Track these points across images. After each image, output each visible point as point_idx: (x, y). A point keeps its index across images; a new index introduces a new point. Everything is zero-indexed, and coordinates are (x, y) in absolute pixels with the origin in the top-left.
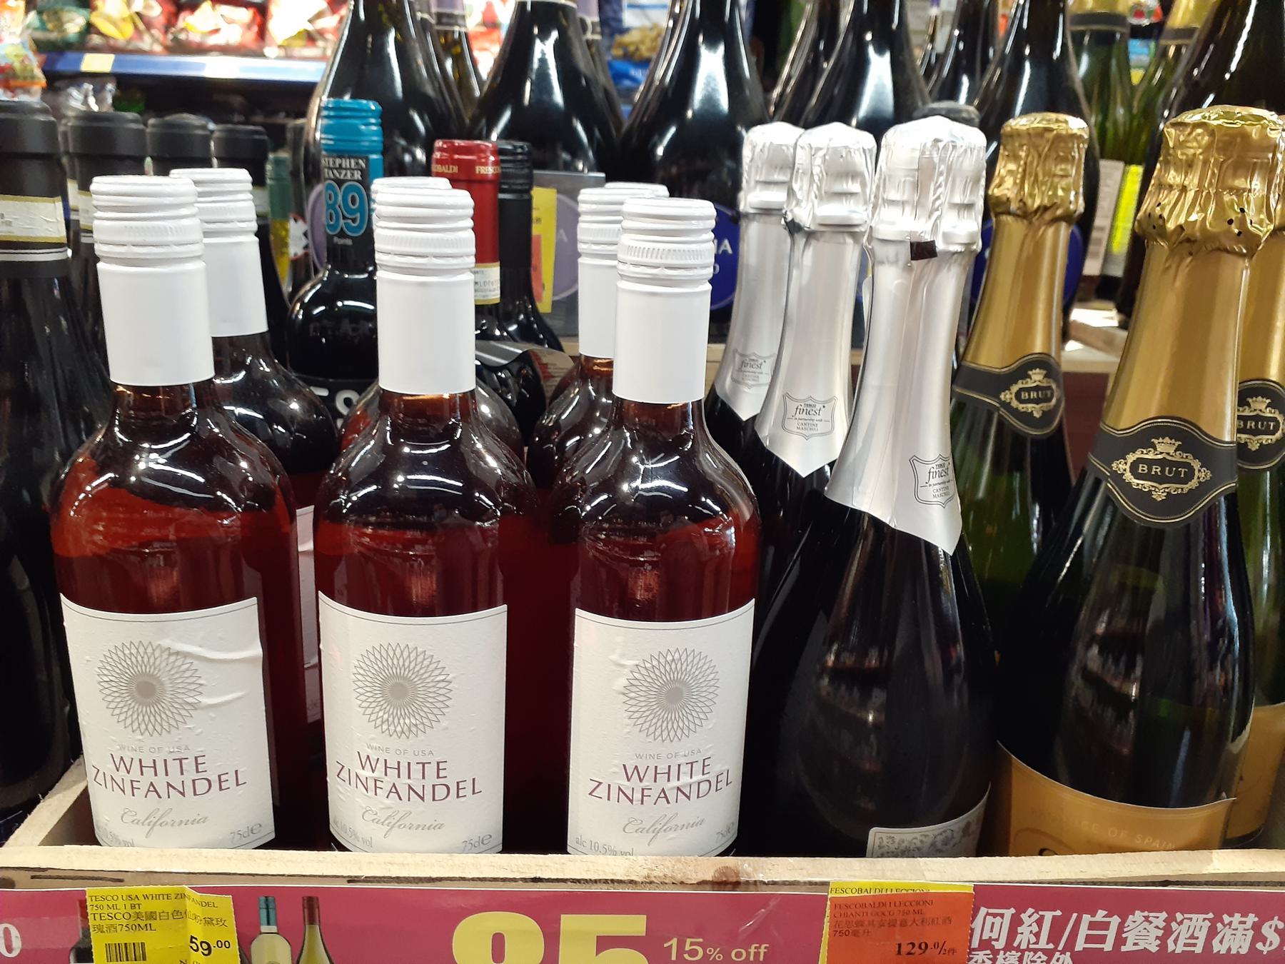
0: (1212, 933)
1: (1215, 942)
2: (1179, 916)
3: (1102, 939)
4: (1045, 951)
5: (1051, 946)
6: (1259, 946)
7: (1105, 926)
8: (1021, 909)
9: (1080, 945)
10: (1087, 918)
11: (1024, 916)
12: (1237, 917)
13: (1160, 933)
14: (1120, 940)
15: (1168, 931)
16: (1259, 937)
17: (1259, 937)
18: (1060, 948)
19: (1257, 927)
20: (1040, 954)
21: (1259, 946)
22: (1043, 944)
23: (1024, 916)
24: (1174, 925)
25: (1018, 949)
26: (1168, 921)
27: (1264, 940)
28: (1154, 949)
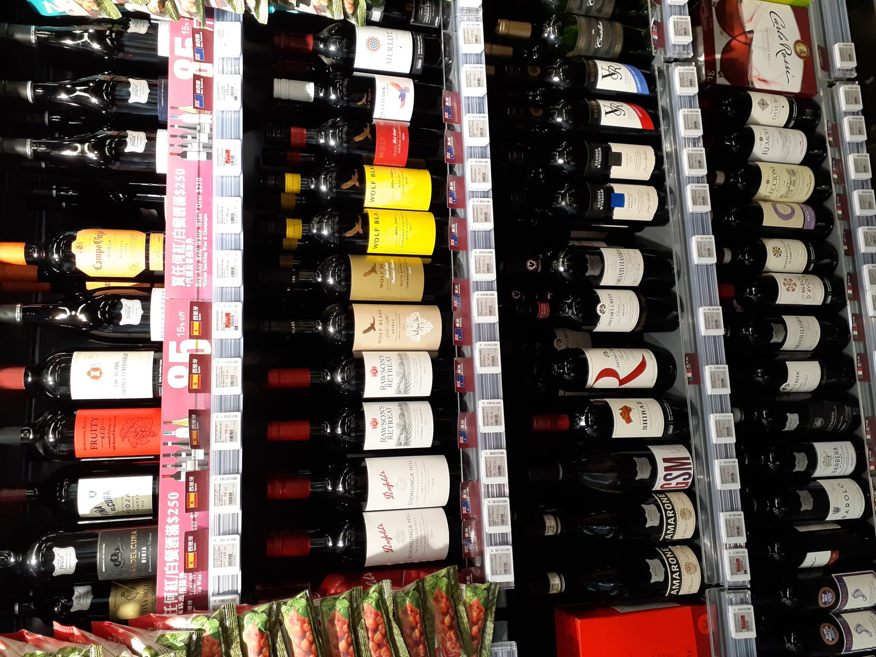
0: (172, 536)
1: (175, 535)
2: (166, 547)
3: (174, 566)
4: (179, 581)
5: (177, 580)
6: (176, 522)
7: (170, 567)
8: (165, 591)
9: (177, 572)
10: (167, 572)
11: (167, 590)
12: (166, 531)
13: (172, 550)
14: (175, 561)
15: (172, 548)
16: (174, 523)
17: (174, 523)
18: (177, 577)
19: (170, 525)
20: (179, 582)
21: (176, 522)
22: (176, 582)
23: (167, 590)
24: (169, 548)
25: (178, 589)
26: (167, 549)
27: (174, 521)
28: (178, 551)
